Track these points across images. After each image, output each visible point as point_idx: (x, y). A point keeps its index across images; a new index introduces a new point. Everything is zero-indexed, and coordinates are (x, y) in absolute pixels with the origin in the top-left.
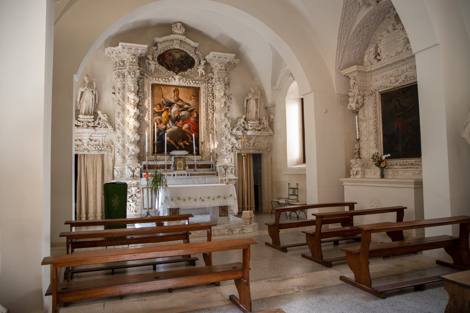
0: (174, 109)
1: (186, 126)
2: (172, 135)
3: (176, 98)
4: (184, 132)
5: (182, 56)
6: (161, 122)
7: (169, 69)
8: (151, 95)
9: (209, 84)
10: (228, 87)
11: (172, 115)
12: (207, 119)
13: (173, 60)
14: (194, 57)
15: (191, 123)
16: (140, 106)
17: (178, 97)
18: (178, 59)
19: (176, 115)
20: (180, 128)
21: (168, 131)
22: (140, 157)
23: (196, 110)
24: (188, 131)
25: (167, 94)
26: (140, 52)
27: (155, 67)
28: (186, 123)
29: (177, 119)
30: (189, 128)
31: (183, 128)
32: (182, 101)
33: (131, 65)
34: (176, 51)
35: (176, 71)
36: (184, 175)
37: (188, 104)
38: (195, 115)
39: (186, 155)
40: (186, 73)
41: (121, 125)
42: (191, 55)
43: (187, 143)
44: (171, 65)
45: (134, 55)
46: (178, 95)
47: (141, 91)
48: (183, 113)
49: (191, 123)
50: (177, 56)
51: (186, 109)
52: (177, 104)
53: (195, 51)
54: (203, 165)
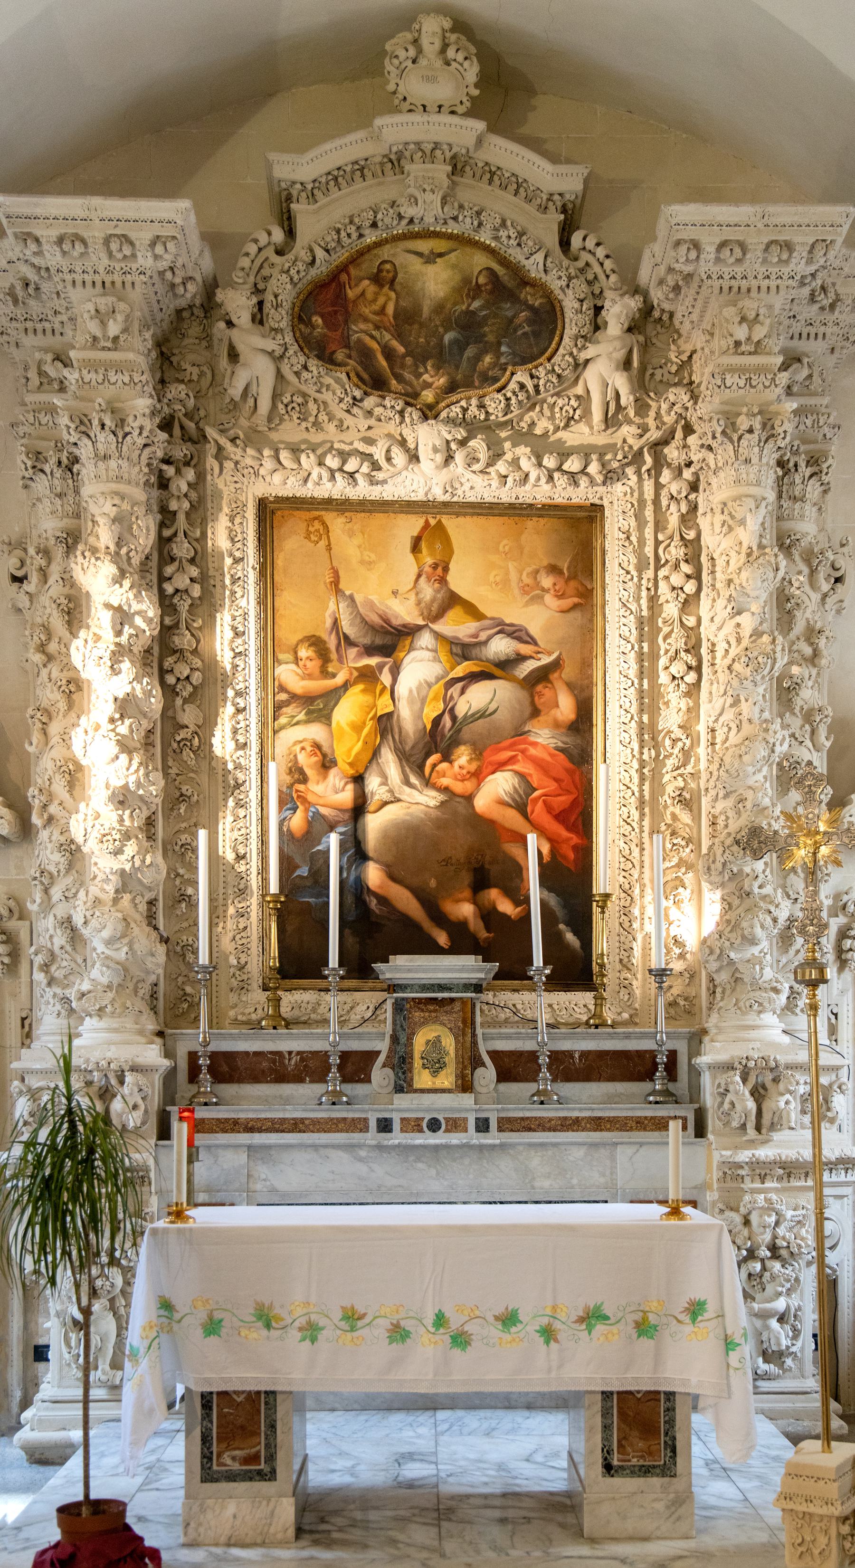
1: (500, 785)
3: (428, 591)
9: (666, 476)
13: (406, 318)
14: (555, 283)
15: (538, 763)
16: (178, 652)
17: (443, 581)
18: (439, 308)
19: (431, 712)
20: (457, 805)
24: (512, 819)
28: (499, 766)
34: (424, 246)
37: (517, 633)
42: (533, 266)
44: (389, 354)
46: (441, 570)
47: (182, 549)
48: (478, 696)
49: (538, 763)
51: (504, 667)
52: (438, 636)
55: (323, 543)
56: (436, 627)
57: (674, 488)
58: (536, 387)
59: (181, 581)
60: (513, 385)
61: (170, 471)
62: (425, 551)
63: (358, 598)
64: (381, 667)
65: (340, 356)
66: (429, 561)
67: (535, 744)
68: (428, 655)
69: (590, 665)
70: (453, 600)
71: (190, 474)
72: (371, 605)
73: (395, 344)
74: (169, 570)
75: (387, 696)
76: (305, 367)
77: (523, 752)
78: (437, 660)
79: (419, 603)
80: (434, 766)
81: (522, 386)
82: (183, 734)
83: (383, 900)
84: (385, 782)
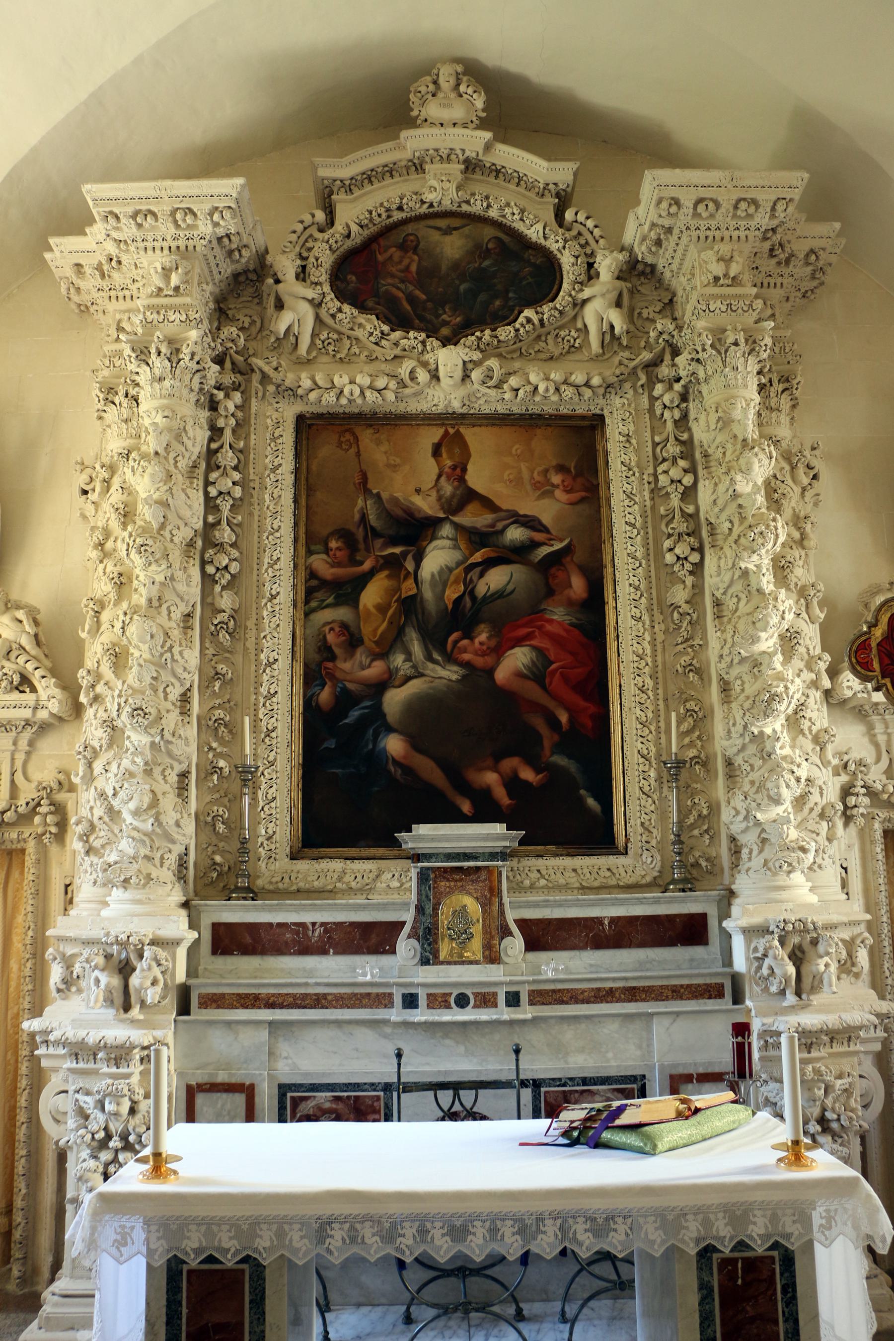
0: (438, 557)
1: (519, 658)
2: (423, 720)
3: (448, 489)
4: (506, 697)
5: (478, 246)
6: (353, 641)
7: (400, 321)
8: (290, 479)
9: (659, 389)
10: (785, 402)
11: (428, 594)
12: (661, 607)
13: (428, 274)
14: (553, 245)
15: (553, 638)
16: (219, 547)
17: (462, 480)
18: (456, 266)
19: (452, 594)
20: (478, 677)
21: (395, 700)
22: (218, 872)
23: (579, 556)
24: (533, 691)
25: (394, 467)
26: (205, 228)
27: (318, 318)
28: (518, 642)
29: (463, 616)
30: (537, 674)
31: (502, 674)
32: (488, 504)
33: (157, 309)
34: (442, 223)
35: (445, 331)
36: (486, 1000)
37: (530, 523)
38: (578, 586)
39: (503, 855)
40: (505, 332)
41: (106, 670)
42: (534, 233)
43: (527, 774)
44: (411, 299)
45: (184, 253)
46: (459, 471)
47: (227, 458)
48: (496, 579)
49: (553, 638)
50: (452, 247)
51: (518, 554)
52: (457, 526)
53: (559, 217)
54: (632, 920)
55: (353, 451)
56: (456, 519)
57: (666, 399)
58: (541, 321)
59: (226, 484)
60: (521, 319)
61: (220, 395)
62: (444, 455)
63: (385, 496)
64: (404, 555)
65: (370, 303)
66: (449, 463)
67: (551, 621)
68: (447, 543)
69: (600, 551)
70: (470, 496)
71: (237, 397)
72: (395, 501)
73: (417, 292)
74: (213, 476)
75: (410, 582)
76: (340, 310)
77: (540, 628)
78: (456, 547)
79: (439, 498)
80: (456, 642)
81: (529, 320)
82: (220, 617)
83: (407, 770)
84: (409, 657)
